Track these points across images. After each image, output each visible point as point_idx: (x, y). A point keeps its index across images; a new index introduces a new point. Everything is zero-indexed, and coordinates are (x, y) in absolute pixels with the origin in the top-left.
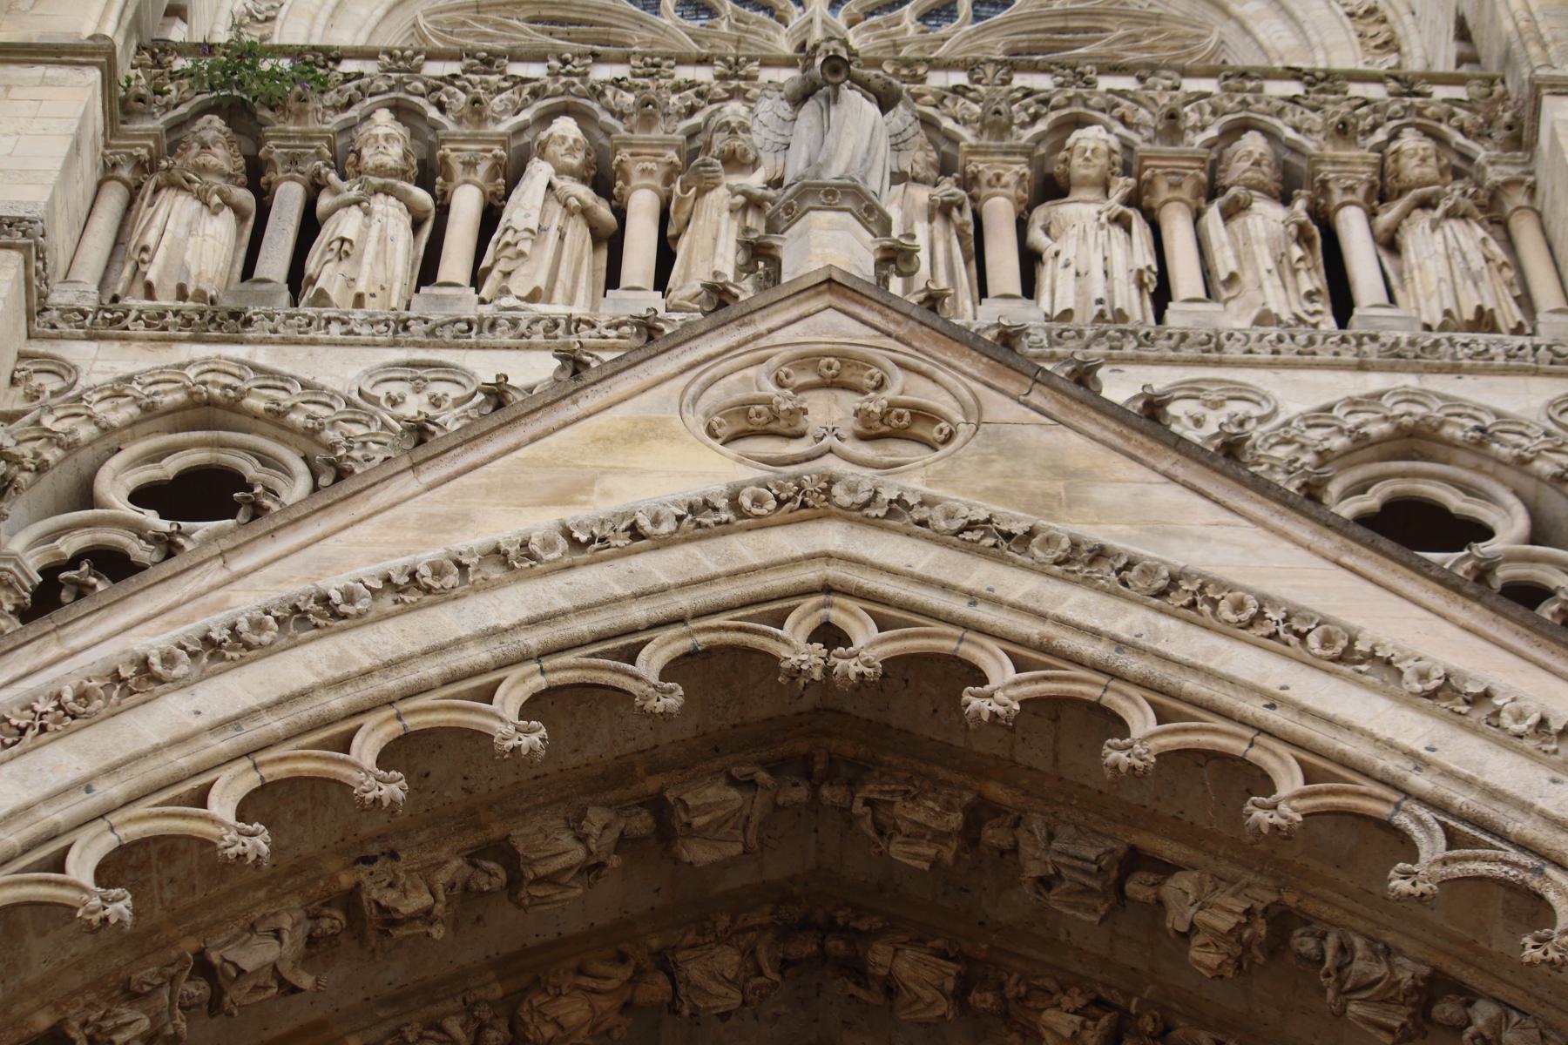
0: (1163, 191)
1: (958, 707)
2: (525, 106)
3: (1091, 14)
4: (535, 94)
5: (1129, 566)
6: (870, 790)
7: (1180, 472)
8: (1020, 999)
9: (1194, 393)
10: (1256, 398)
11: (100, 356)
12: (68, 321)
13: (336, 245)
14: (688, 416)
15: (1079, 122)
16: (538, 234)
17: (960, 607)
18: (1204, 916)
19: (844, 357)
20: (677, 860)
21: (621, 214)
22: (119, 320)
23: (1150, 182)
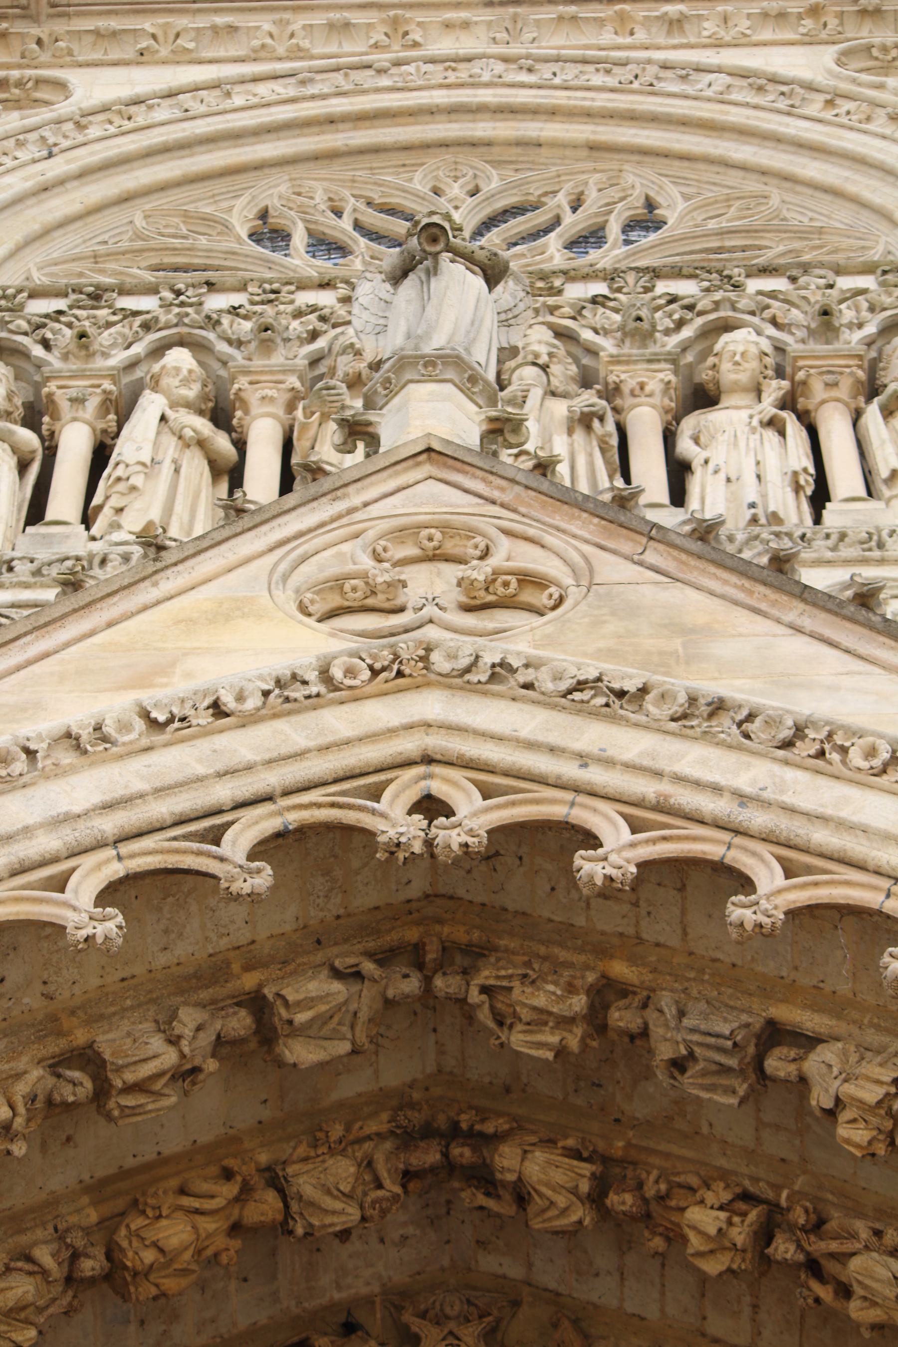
0: (818, 390)
1: (569, 872)
2: (136, 339)
3: (748, 231)
4: (147, 327)
5: (750, 717)
6: (486, 975)
7: (807, 623)
8: (661, 1198)
14: (278, 593)
15: (727, 327)
16: (151, 467)
17: (570, 770)
18: (849, 1089)
19: (445, 527)
20: (280, 1063)
21: (241, 446)
23: (804, 383)
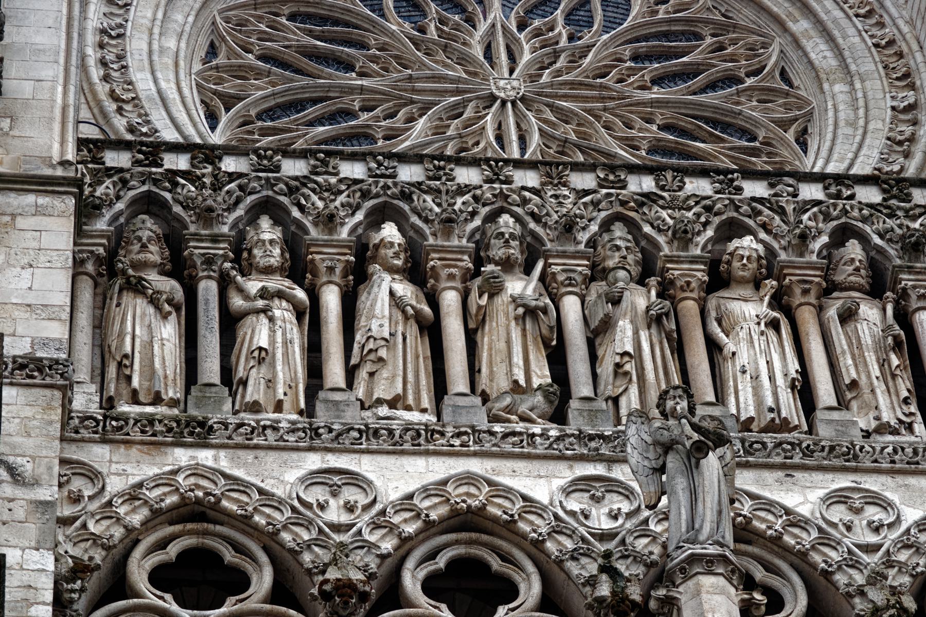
0: (798, 299)
2: (358, 207)
3: (687, 21)
9: (843, 499)
10: (885, 505)
11: (114, 459)
12: (86, 428)
13: (256, 354)
22: (121, 428)
23: (789, 287)
